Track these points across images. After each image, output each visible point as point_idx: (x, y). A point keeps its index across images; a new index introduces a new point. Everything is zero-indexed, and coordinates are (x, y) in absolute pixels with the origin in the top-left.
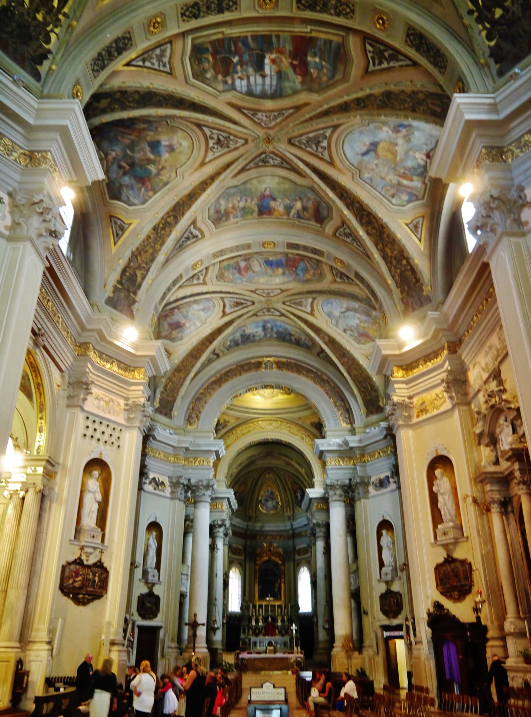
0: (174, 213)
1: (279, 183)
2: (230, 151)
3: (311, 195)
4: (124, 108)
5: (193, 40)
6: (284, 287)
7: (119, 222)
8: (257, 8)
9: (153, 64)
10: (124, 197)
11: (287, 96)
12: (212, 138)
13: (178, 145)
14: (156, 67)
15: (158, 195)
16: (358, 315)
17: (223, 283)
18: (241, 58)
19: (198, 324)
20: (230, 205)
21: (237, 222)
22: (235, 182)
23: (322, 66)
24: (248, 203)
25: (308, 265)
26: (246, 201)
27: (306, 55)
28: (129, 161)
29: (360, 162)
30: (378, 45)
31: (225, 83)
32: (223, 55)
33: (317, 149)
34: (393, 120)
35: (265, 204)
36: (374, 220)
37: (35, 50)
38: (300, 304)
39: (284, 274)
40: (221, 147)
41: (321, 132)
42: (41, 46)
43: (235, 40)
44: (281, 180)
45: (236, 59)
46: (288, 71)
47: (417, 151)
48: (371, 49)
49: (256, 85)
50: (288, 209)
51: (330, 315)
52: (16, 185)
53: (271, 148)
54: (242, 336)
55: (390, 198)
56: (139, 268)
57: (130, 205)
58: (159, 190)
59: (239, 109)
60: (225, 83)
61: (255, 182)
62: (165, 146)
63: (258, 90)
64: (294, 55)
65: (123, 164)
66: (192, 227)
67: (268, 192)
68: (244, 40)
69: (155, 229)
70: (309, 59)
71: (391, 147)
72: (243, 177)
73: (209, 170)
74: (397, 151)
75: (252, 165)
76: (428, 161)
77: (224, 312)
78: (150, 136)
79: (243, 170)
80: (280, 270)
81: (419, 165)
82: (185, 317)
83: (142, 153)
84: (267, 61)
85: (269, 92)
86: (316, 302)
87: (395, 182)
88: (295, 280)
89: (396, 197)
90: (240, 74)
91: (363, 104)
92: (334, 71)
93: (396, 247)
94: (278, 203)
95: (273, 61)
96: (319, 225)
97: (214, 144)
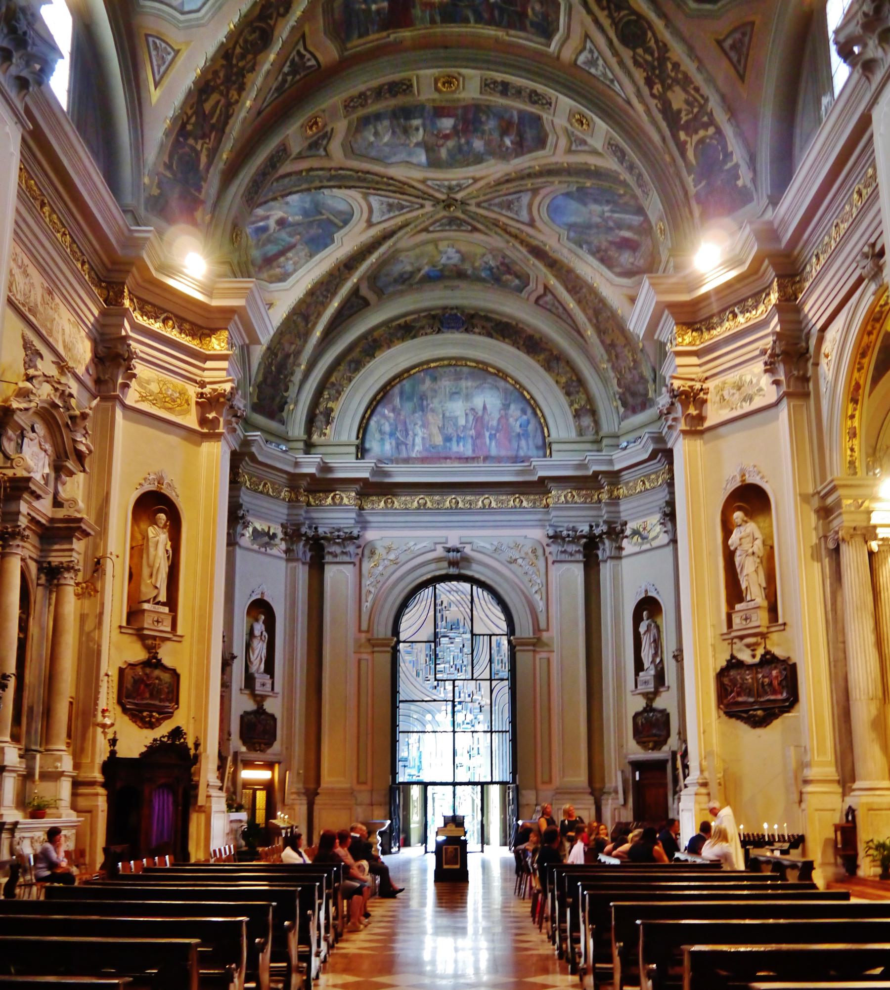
5: (549, 46)
8: (461, 79)
14: (601, 62)
43: (491, 22)
68: (479, 19)
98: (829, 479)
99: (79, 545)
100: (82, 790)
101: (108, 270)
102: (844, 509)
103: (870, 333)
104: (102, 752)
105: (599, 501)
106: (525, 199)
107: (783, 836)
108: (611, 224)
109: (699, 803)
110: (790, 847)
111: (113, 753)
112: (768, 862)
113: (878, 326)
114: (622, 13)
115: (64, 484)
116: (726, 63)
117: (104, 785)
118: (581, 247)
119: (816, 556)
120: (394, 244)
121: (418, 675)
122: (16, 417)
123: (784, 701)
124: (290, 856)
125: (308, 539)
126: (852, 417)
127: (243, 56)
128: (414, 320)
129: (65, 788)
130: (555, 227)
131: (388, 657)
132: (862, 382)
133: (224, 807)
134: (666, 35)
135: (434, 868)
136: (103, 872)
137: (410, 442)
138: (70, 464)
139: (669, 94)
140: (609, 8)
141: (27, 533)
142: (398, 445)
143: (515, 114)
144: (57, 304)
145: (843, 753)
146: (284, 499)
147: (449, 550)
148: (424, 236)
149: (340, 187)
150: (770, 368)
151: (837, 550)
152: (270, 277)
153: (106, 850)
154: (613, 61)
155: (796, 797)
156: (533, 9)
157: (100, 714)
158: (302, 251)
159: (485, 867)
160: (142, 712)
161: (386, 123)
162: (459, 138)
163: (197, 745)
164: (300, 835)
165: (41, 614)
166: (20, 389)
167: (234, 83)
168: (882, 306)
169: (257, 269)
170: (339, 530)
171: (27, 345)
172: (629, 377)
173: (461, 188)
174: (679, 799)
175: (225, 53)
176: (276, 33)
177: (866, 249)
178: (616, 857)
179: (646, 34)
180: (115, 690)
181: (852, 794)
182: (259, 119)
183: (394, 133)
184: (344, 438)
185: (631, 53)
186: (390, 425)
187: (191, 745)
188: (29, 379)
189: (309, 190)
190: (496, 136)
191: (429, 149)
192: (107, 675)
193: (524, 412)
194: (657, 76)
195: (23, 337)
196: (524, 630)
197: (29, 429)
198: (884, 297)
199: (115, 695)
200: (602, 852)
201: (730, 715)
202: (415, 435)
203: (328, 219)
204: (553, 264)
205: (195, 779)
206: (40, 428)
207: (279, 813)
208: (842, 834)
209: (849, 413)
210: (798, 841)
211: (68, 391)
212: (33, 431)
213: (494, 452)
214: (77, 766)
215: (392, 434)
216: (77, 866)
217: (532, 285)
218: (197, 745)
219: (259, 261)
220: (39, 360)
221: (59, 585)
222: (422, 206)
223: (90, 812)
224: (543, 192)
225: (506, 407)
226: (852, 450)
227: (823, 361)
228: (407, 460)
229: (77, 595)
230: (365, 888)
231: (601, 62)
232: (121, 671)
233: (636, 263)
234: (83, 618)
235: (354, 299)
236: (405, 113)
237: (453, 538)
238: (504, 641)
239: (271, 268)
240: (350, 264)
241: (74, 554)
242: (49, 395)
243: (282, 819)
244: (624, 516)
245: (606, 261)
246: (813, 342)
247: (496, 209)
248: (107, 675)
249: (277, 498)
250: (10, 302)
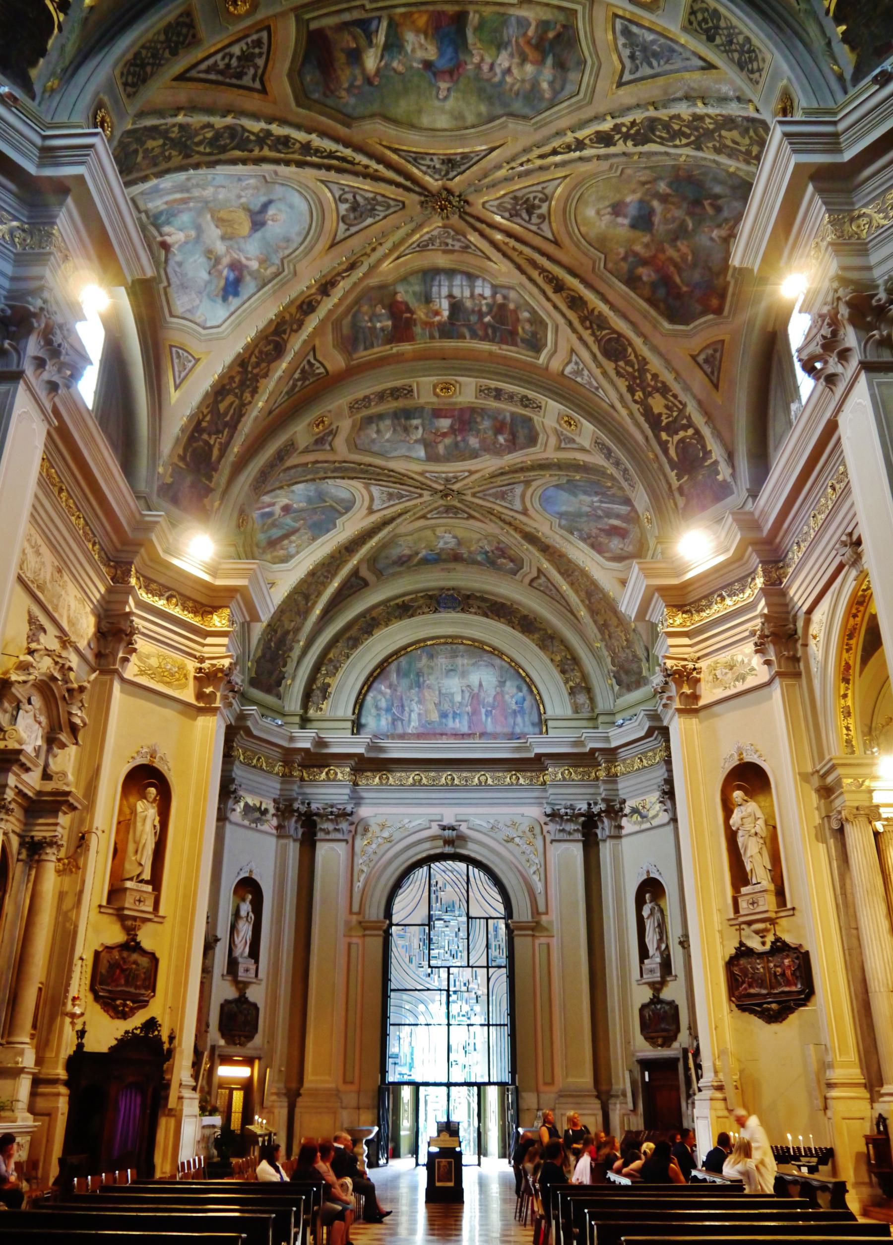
1: (420, 111)
3: (349, 100)
11: (413, 273)
12: (542, 217)
13: (602, 212)
14: (586, 372)
20: (529, 68)
23: (371, 320)
24: (488, 60)
27: (394, 326)
28: (698, 210)
31: (505, 297)
33: (354, 197)
40: (528, 199)
41: (353, 230)
43: (485, 338)
46: (416, 305)
47: (186, 243)
50: (394, 45)
60: (505, 297)
61: (470, 119)
62: (625, 216)
63: (458, 280)
65: (710, 211)
66: (627, 77)
67: (443, 85)
68: (474, 335)
70: (389, 323)
71: (229, 230)
74: (217, 227)
76: (159, 239)
78: (641, 244)
81: (168, 223)
84: (446, 314)
90: (484, 302)
91: (305, 307)
94: (420, 54)
95: (437, 313)
96: (313, 26)
97: (540, 207)
98: (827, 758)
99: (64, 820)
100: (42, 1090)
101: (117, 550)
102: (845, 789)
103: (855, 616)
104: (67, 1045)
105: (597, 778)
106: (519, 490)
107: (810, 1149)
108: (600, 513)
109: (715, 1110)
110: (819, 1163)
111: (80, 1046)
112: (795, 1182)
113: (862, 609)
114: (604, 332)
115: (55, 756)
116: (700, 375)
117: (67, 1084)
119: (820, 837)
120: (394, 529)
121: (411, 961)
122: (13, 690)
123: (799, 993)
124: (266, 1171)
125: (300, 815)
126: (845, 696)
127: (257, 365)
128: (412, 600)
129: (24, 1086)
130: (548, 516)
131: (380, 940)
132: (851, 663)
133: (197, 1110)
134: (645, 351)
135: (425, 1186)
136: (55, 1188)
137: (406, 718)
138: (63, 737)
139: (650, 400)
140: (591, 327)
141: (13, 806)
142: (394, 721)
143: (508, 415)
144: (65, 582)
145: (867, 1052)
146: (277, 774)
147: (444, 828)
148: (422, 523)
149: (343, 478)
150: (760, 649)
151: (841, 831)
152: (273, 558)
153: (61, 1161)
154: (597, 372)
155: (820, 1103)
156: (523, 329)
157: (70, 1002)
158: (305, 535)
159: (482, 1184)
160: (115, 1000)
161: (388, 422)
163: (172, 1038)
164: (278, 1146)
165: (18, 890)
166: (21, 662)
167: (248, 387)
168: (864, 590)
170: (332, 806)
171: (32, 620)
172: (622, 655)
173: (457, 479)
174: (693, 1103)
175: (241, 362)
176: (289, 346)
177: (844, 538)
178: (627, 1175)
179: (626, 350)
180: (89, 976)
181: (882, 1099)
182: (271, 417)
183: (395, 430)
184: (340, 713)
185: (613, 365)
186: (387, 700)
187: (165, 1038)
188: (31, 652)
189: (313, 480)
190: (490, 433)
191: (427, 445)
192: (81, 959)
193: (519, 689)
194: (638, 385)
195: (29, 612)
196: (523, 913)
197: (25, 701)
198: (866, 583)
199: (88, 982)
200: (611, 1169)
201: (743, 1008)
202: (411, 711)
203: (331, 506)
204: (546, 549)
205: (167, 1077)
206: (37, 700)
207: (256, 1117)
208: (874, 1147)
209: (842, 693)
210: (827, 1156)
211: (68, 664)
212: (30, 703)
213: (490, 728)
214: (39, 1062)
215: (388, 710)
216: (28, 1181)
217: (526, 569)
218: (172, 1038)
219: (263, 544)
220: (42, 634)
221: (39, 861)
222: (421, 496)
223: (49, 1115)
224: (535, 484)
225: (502, 683)
226: (848, 729)
227: (812, 642)
228: (402, 736)
229: (58, 872)
230: (348, 1212)
231: (586, 372)
232: (97, 954)
234: (61, 896)
235: (353, 579)
236: (407, 414)
237: (449, 815)
238: (502, 925)
240: (350, 547)
241: (59, 828)
242: (48, 668)
243: (259, 1124)
244: (622, 794)
245: (597, 547)
246: (800, 624)
247: (491, 499)
248: (81, 959)
249: (271, 773)
250: (20, 579)
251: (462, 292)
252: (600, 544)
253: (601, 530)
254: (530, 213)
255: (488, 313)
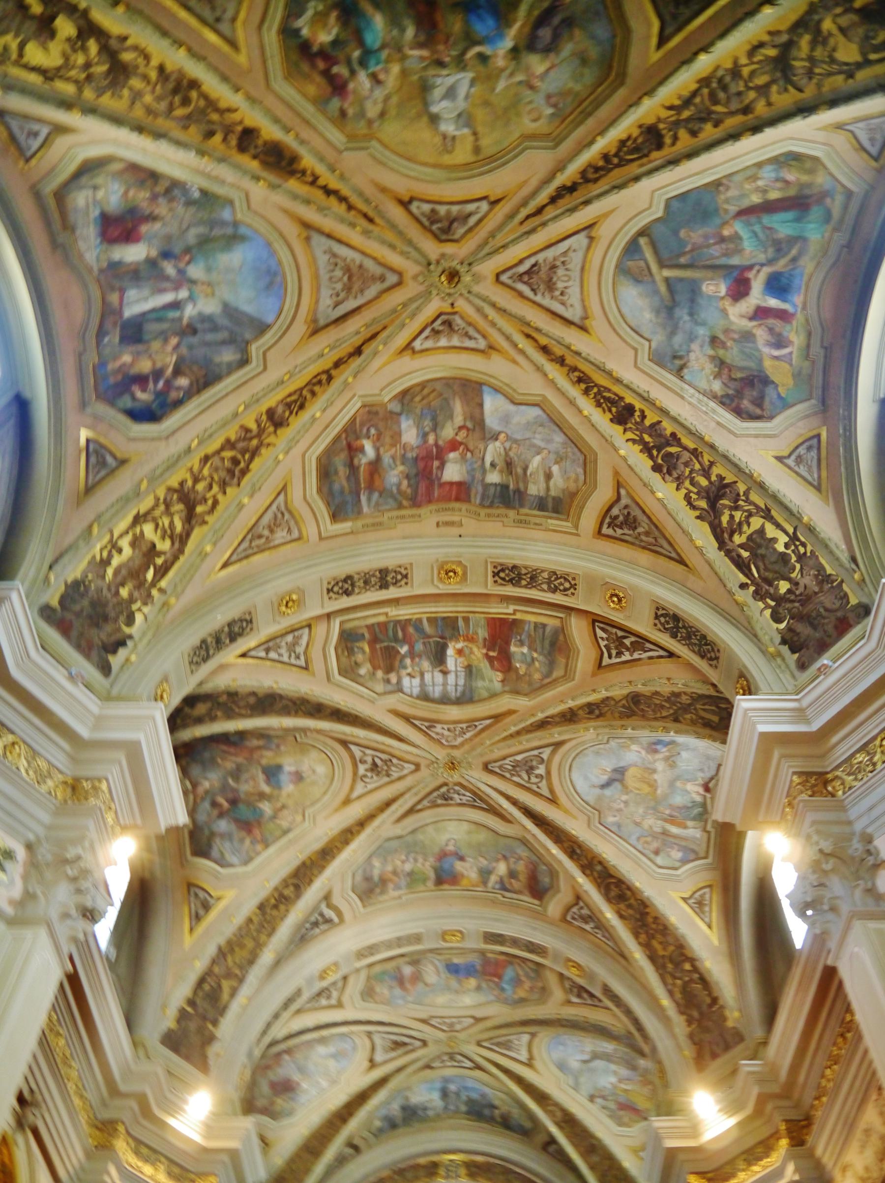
0: (295, 881)
1: (469, 832)
2: (392, 782)
3: (523, 852)
4: (230, 715)
5: (341, 623)
6: (479, 1014)
7: (202, 894)
9: (280, 655)
10: (215, 853)
11: (481, 700)
12: (363, 762)
14: (285, 658)
15: (272, 850)
16: (613, 1067)
17: (372, 1005)
18: (412, 648)
19: (324, 1084)
20: (389, 868)
21: (400, 897)
22: (398, 830)
23: (533, 659)
24: (419, 865)
25: (521, 972)
26: (416, 860)
27: (508, 643)
28: (230, 796)
29: (600, 798)
30: (614, 630)
31: (388, 681)
32: (386, 644)
34: (646, 735)
35: (446, 866)
36: (628, 893)
37: (110, 635)
38: (507, 1045)
39: (478, 988)
40: (377, 775)
41: (536, 752)
42: (119, 630)
43: (404, 624)
44: (473, 827)
45: (404, 650)
46: (482, 665)
47: (688, 781)
48: (604, 635)
49: (434, 685)
50: (485, 874)
51: (562, 1066)
52: (41, 831)
53: (456, 778)
54: (404, 1108)
55: (652, 856)
56: (229, 975)
57: (222, 866)
58: (274, 842)
59: (407, 719)
61: (430, 829)
62: (290, 773)
63: (437, 692)
64: (490, 644)
65: (221, 800)
67: (451, 848)
68: (417, 624)
69: (261, 907)
70: (513, 649)
71: (646, 775)
72: (412, 822)
73: (356, 811)
74: (655, 781)
75: (425, 803)
76: (708, 795)
77: (371, 1060)
78: (268, 757)
79: (411, 811)
80: (472, 982)
82: (301, 1070)
83: (251, 783)
84: (450, 652)
85: (453, 695)
86: (536, 1041)
87: (658, 830)
88: (499, 1000)
89: (662, 854)
90: (409, 670)
91: (597, 712)
92: (551, 664)
93: (670, 940)
94: (467, 865)
95: (460, 652)
96: (536, 902)
97: (366, 770)
108: (169, 269)
118: (204, 192)
143: (365, 509)
152: (811, 172)
156: (364, 652)
161: (535, 489)
162: (436, 445)
169: (828, 201)
183: (525, 469)
190: (386, 459)
219: (816, 212)
233: (90, 193)
239: (802, 186)
251: (433, 677)
252: (141, 184)
253: (152, 218)
254: (375, 764)
255: (404, 657)
